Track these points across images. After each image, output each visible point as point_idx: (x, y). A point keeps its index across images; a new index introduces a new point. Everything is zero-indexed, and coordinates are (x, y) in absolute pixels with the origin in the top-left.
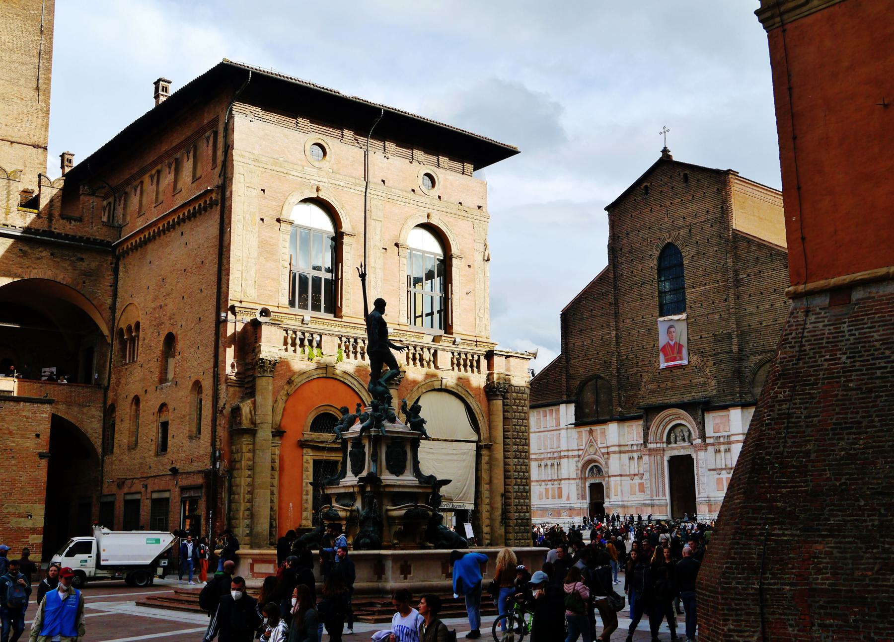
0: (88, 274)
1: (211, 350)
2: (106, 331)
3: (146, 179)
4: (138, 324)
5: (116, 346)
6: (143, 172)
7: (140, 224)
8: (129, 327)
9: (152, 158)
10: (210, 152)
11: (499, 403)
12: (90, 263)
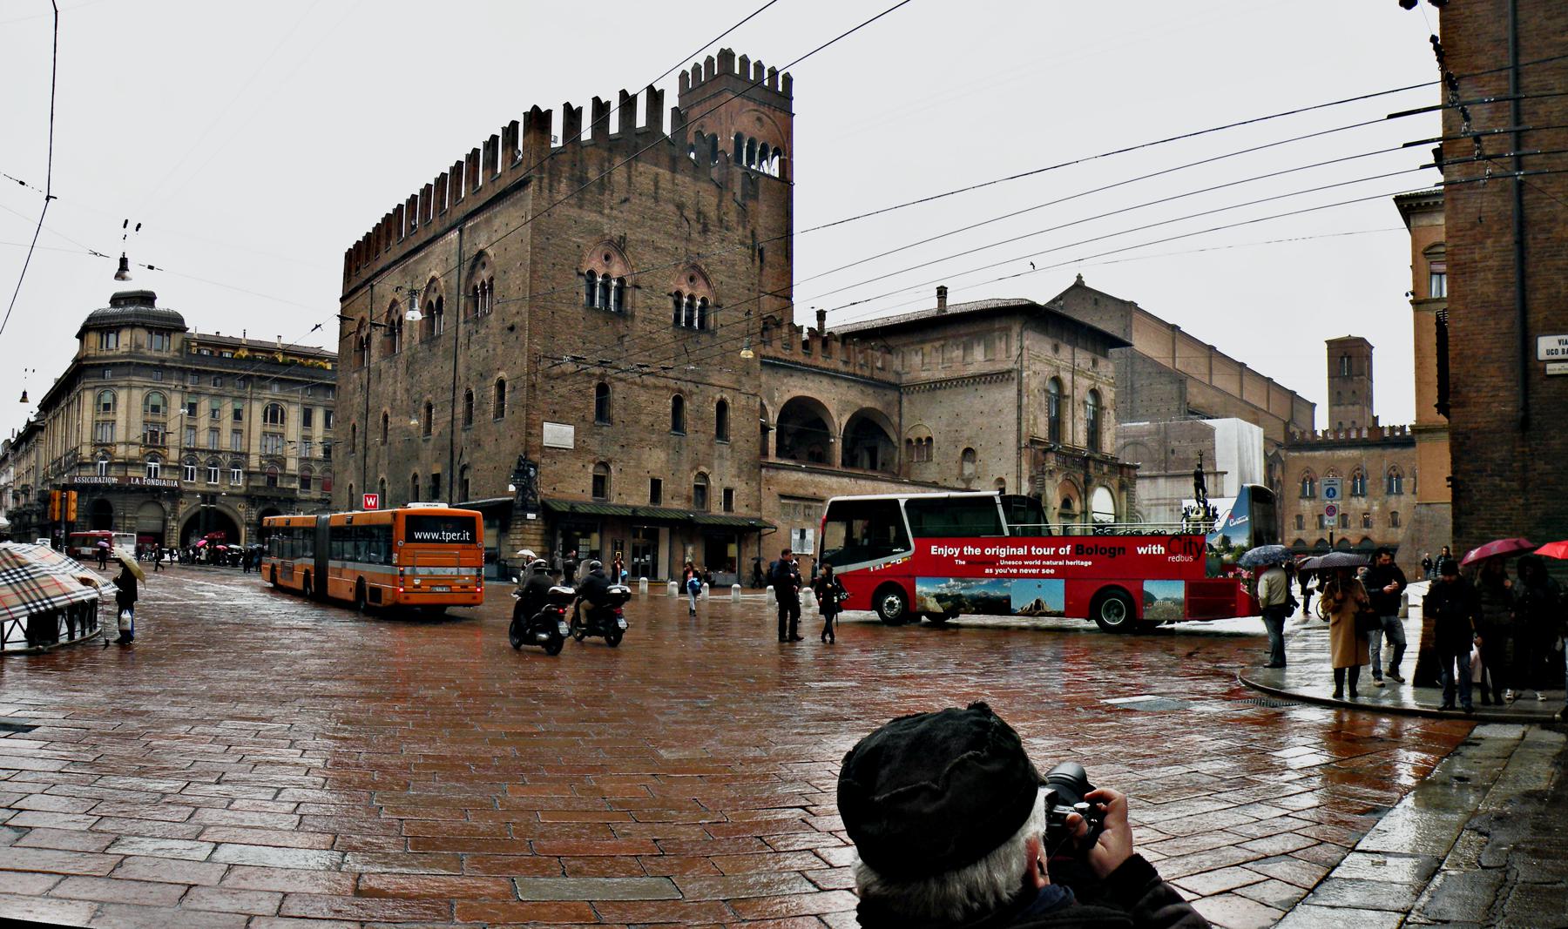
0: (888, 404)
1: (1014, 462)
2: (894, 438)
3: (928, 347)
4: (929, 439)
5: (903, 446)
6: (923, 342)
7: (924, 375)
8: (919, 440)
9: (935, 335)
10: (1003, 346)
11: (1124, 494)
12: (892, 396)
